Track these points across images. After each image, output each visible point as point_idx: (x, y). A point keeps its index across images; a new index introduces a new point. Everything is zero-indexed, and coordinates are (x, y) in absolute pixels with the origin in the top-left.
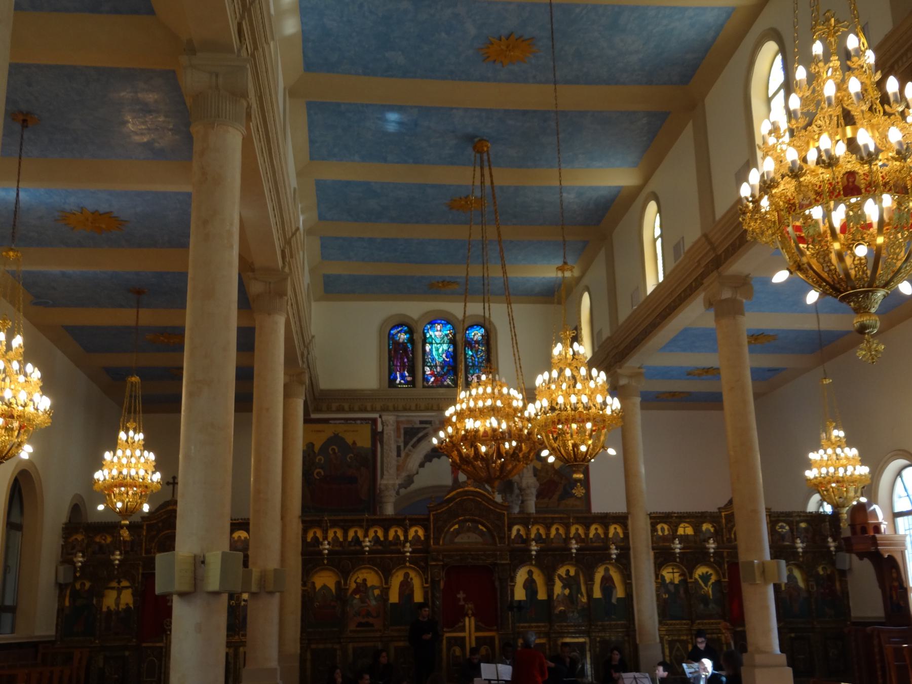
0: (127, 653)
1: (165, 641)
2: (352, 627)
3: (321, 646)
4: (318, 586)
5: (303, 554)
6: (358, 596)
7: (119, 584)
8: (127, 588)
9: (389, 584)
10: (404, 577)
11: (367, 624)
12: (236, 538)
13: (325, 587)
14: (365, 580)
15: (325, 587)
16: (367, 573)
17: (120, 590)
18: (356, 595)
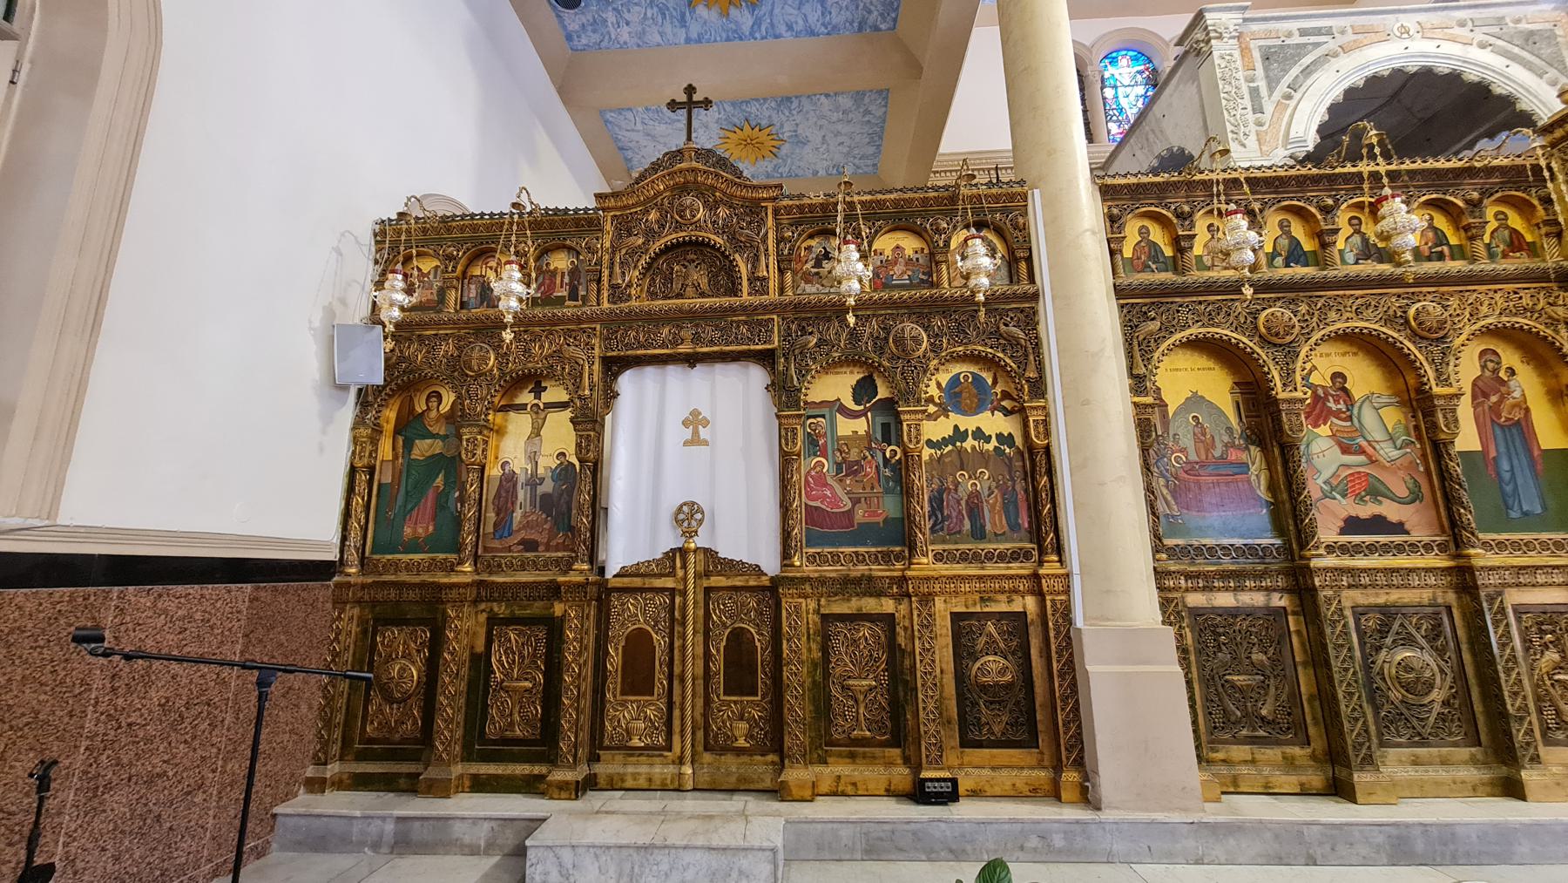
0: (558, 609)
1: (680, 573)
2: (1328, 533)
3: (1225, 600)
4: (1174, 399)
5: (1120, 292)
6: (1324, 430)
7: (538, 397)
8: (563, 406)
9: (1454, 384)
10: (1484, 367)
11: (1378, 524)
12: (888, 252)
13: (1195, 400)
14: (1338, 377)
15: (1195, 400)
16: (1344, 354)
17: (540, 412)
18: (1316, 425)
